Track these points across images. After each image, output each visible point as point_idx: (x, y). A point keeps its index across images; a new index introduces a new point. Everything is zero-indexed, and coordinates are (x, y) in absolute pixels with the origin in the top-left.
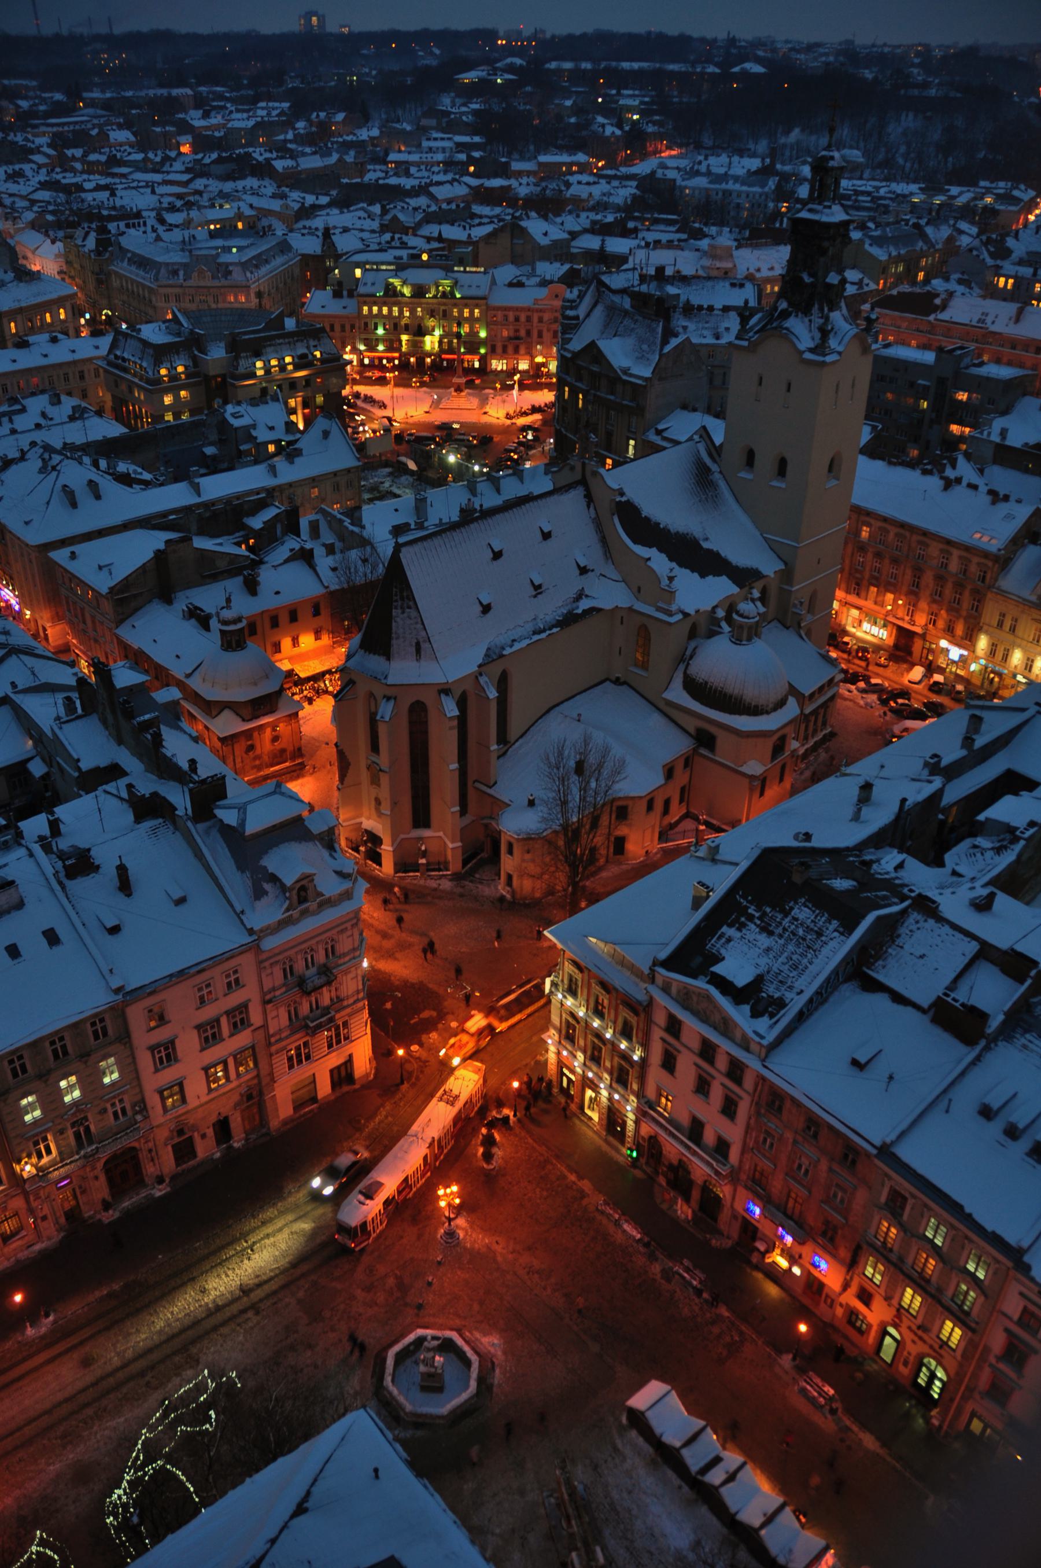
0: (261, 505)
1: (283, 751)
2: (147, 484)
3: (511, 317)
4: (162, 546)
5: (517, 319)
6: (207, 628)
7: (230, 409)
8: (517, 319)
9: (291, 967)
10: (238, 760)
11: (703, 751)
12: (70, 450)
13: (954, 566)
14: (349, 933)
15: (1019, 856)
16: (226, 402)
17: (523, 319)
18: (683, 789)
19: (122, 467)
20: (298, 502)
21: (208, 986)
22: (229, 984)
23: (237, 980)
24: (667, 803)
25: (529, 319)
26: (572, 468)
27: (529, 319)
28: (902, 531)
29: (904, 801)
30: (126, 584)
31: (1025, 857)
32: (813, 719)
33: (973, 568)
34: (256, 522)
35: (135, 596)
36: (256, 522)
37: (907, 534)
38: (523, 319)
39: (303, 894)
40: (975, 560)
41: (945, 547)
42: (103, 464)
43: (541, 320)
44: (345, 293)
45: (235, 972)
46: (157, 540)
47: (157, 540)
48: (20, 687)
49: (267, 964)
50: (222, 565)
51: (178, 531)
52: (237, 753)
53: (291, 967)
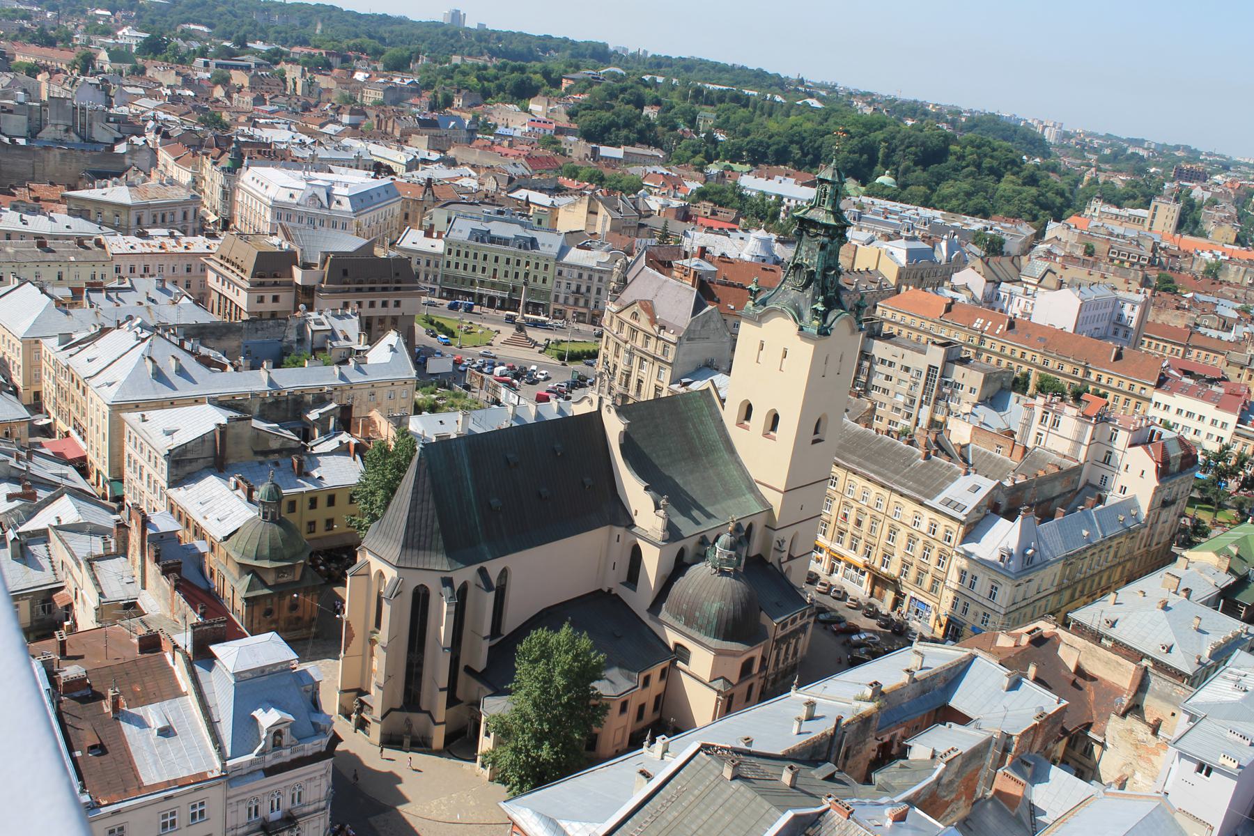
0: (321, 400)
1: (299, 619)
2: (223, 367)
3: (576, 273)
4: (224, 421)
5: (580, 276)
6: (250, 499)
7: (314, 315)
8: (580, 276)
9: (256, 808)
10: (256, 621)
11: (680, 664)
12: (160, 329)
13: (924, 527)
14: (317, 782)
15: (939, 778)
16: (310, 308)
17: (585, 276)
18: (658, 698)
19: (204, 351)
20: (356, 404)
21: (173, 814)
22: (194, 816)
23: (202, 812)
24: (642, 708)
25: (590, 278)
26: (591, 402)
27: (590, 278)
28: (881, 490)
29: (839, 720)
30: (184, 449)
31: (945, 781)
32: (784, 647)
33: (940, 531)
34: (313, 415)
35: (191, 461)
36: (313, 415)
37: (886, 493)
38: (585, 276)
39: (278, 738)
40: (943, 522)
41: (918, 508)
42: (188, 346)
43: (600, 279)
44: (435, 235)
45: (202, 804)
46: (221, 417)
47: (221, 417)
48: (63, 523)
49: (233, 800)
50: (275, 445)
51: (242, 411)
52: (256, 613)
53: (256, 808)
